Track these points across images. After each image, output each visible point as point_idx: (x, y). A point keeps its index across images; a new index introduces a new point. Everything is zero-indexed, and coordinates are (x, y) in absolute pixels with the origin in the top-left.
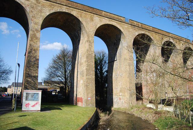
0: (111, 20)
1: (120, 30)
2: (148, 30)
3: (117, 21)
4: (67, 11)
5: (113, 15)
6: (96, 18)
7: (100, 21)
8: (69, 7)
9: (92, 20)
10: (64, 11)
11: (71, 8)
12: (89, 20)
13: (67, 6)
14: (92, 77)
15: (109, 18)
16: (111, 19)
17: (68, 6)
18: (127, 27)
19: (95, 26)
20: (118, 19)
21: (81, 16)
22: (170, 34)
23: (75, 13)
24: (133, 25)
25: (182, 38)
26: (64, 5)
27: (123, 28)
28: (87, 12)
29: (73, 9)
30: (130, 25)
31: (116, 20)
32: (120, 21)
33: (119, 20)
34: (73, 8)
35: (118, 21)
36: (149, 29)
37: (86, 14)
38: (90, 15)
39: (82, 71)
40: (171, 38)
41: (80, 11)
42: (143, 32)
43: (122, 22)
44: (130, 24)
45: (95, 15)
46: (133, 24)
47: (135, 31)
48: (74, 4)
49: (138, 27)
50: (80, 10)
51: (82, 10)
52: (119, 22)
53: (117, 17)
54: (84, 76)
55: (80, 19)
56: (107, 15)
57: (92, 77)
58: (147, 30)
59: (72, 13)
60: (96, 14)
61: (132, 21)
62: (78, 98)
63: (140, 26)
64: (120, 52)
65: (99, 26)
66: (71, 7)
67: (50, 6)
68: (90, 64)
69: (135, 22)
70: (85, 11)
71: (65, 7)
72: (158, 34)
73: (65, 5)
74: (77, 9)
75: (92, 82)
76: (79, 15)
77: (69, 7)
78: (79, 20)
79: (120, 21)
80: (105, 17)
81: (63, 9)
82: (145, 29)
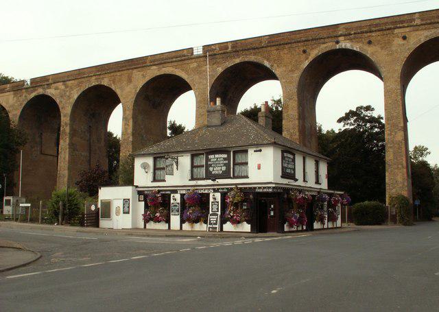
0: (161, 66)
9: (130, 80)
10: (93, 84)
18: (195, 65)
27: (187, 72)
31: (172, 62)
32: (181, 61)
40: (341, 39)
41: (112, 74)
42: (237, 61)
43: (185, 60)
45: (135, 71)
47: (215, 66)
52: (179, 63)
55: (113, 87)
58: (249, 49)
60: (135, 68)
67: (78, 85)
72: (287, 46)
79: (181, 61)
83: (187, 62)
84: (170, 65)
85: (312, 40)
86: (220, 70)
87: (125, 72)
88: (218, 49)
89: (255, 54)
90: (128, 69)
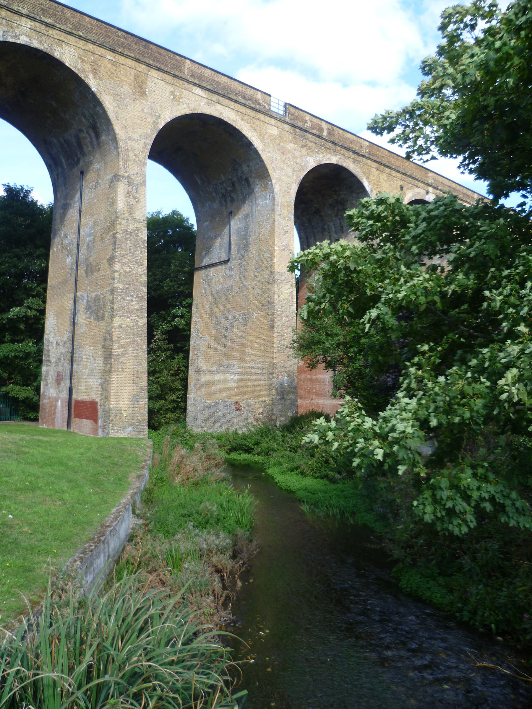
0: (215, 97)
1: (249, 144)
2: (354, 152)
3: (241, 104)
4: (35, 44)
5: (225, 79)
6: (157, 84)
7: (176, 99)
8: (47, 25)
9: (140, 89)
10: (23, 40)
11: (52, 32)
12: (127, 89)
13: (34, 19)
14: (136, 322)
15: (209, 90)
16: (218, 94)
17: (42, 22)
18: (274, 131)
19: (150, 120)
20: (244, 98)
21: (95, 72)
22: (431, 174)
23: (69, 54)
24: (301, 129)
25: (470, 193)
26: (21, 15)
27: (261, 136)
28: (122, 54)
29: (63, 36)
30: (287, 127)
31: (236, 102)
33: (248, 103)
34: (60, 30)
35: (245, 105)
36: (356, 148)
37: (115, 64)
38: (133, 72)
39: (97, 299)
41: (90, 46)
42: (334, 160)
43: (259, 111)
44: (288, 120)
45: (154, 73)
46: (300, 124)
47: (304, 151)
48: (69, 13)
49: (319, 137)
50: (94, 43)
51: (101, 46)
52: (249, 111)
53: (239, 88)
54: (103, 318)
56: (201, 77)
57: (136, 322)
58: (348, 149)
59: (57, 55)
60: (159, 69)
61: (297, 113)
62: (77, 402)
63: (325, 133)
64: (246, 228)
65: (167, 117)
66: (52, 26)
68: (128, 269)
69: (308, 118)
70: (113, 51)
71: (30, 23)
72: (388, 170)
73: (28, 17)
74: (80, 37)
75: (135, 341)
76: (87, 67)
77: (47, 25)
78: (87, 87)
80: (195, 84)
81: (17, 31)
82: (345, 148)
83: (262, 117)
84: (232, 104)
85: (409, 176)
86: (312, 163)
87: (129, 62)
88: (309, 124)
89: (354, 161)
90: (137, 60)
